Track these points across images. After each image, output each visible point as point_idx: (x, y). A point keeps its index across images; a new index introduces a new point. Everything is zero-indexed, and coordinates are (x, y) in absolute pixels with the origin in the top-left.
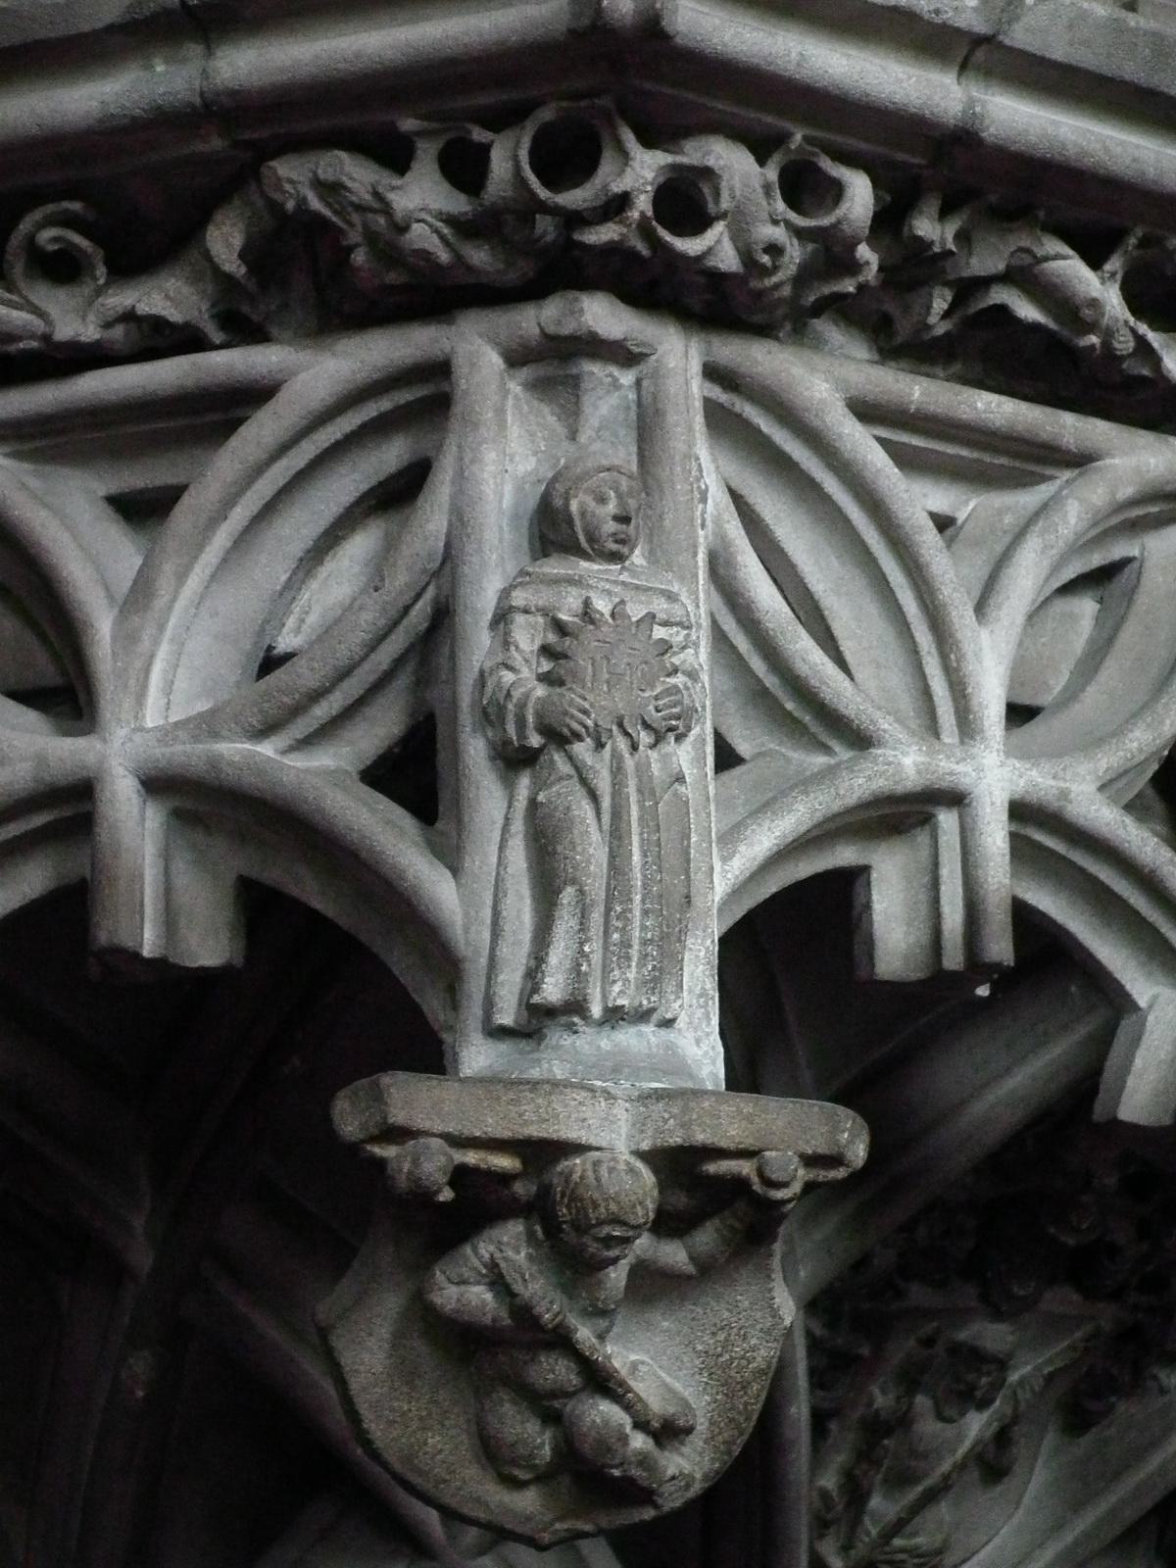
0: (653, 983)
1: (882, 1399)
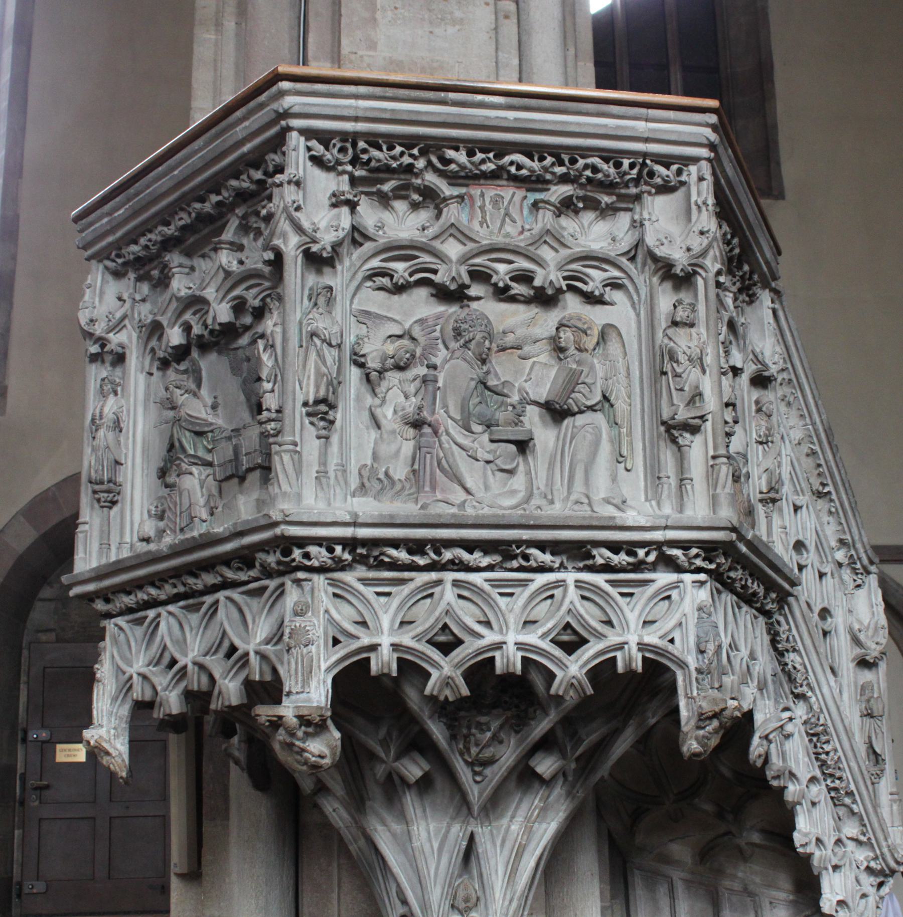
0: (303, 687)
1: (465, 731)
